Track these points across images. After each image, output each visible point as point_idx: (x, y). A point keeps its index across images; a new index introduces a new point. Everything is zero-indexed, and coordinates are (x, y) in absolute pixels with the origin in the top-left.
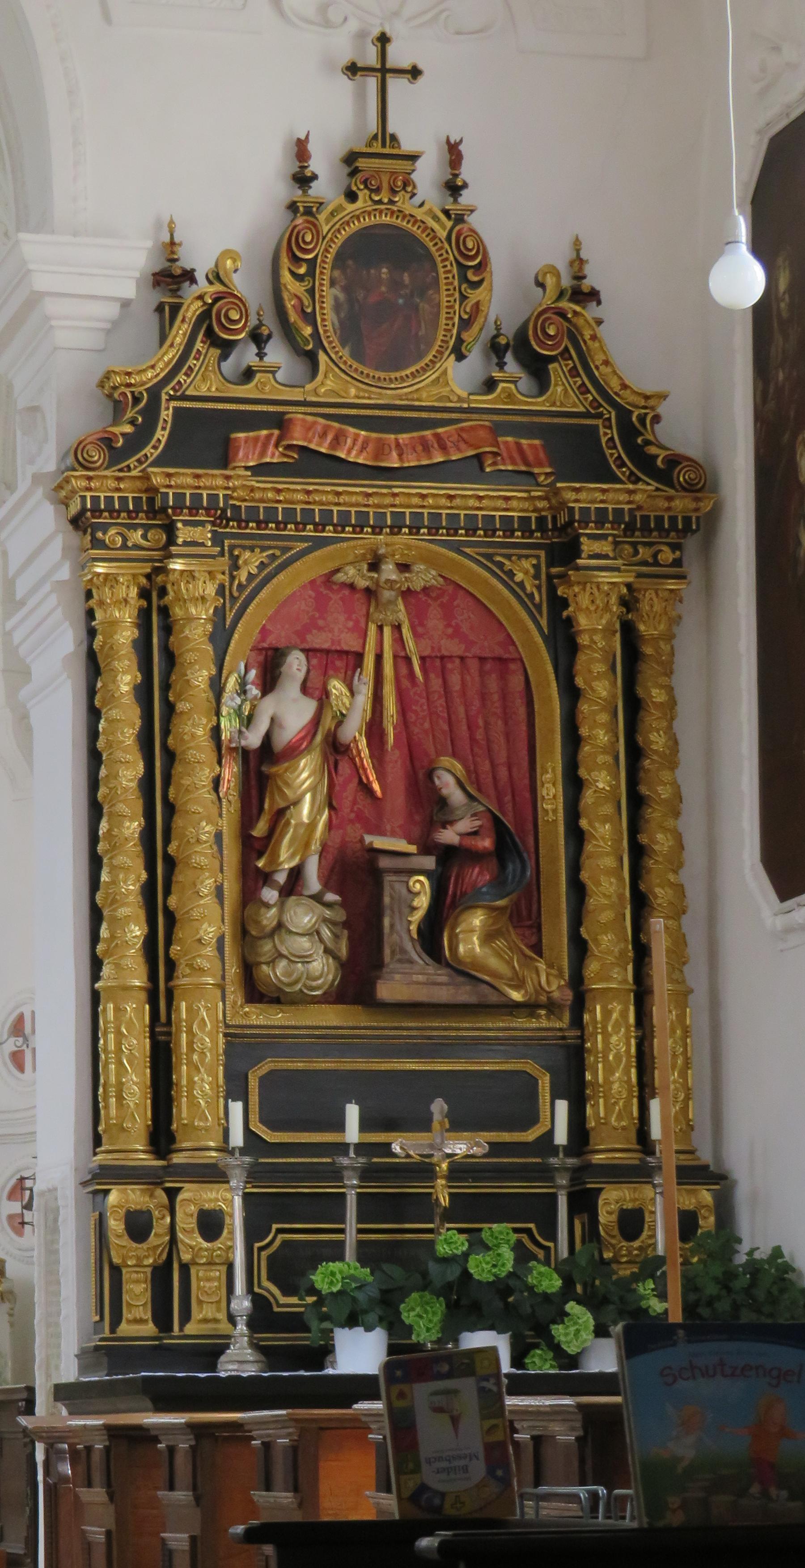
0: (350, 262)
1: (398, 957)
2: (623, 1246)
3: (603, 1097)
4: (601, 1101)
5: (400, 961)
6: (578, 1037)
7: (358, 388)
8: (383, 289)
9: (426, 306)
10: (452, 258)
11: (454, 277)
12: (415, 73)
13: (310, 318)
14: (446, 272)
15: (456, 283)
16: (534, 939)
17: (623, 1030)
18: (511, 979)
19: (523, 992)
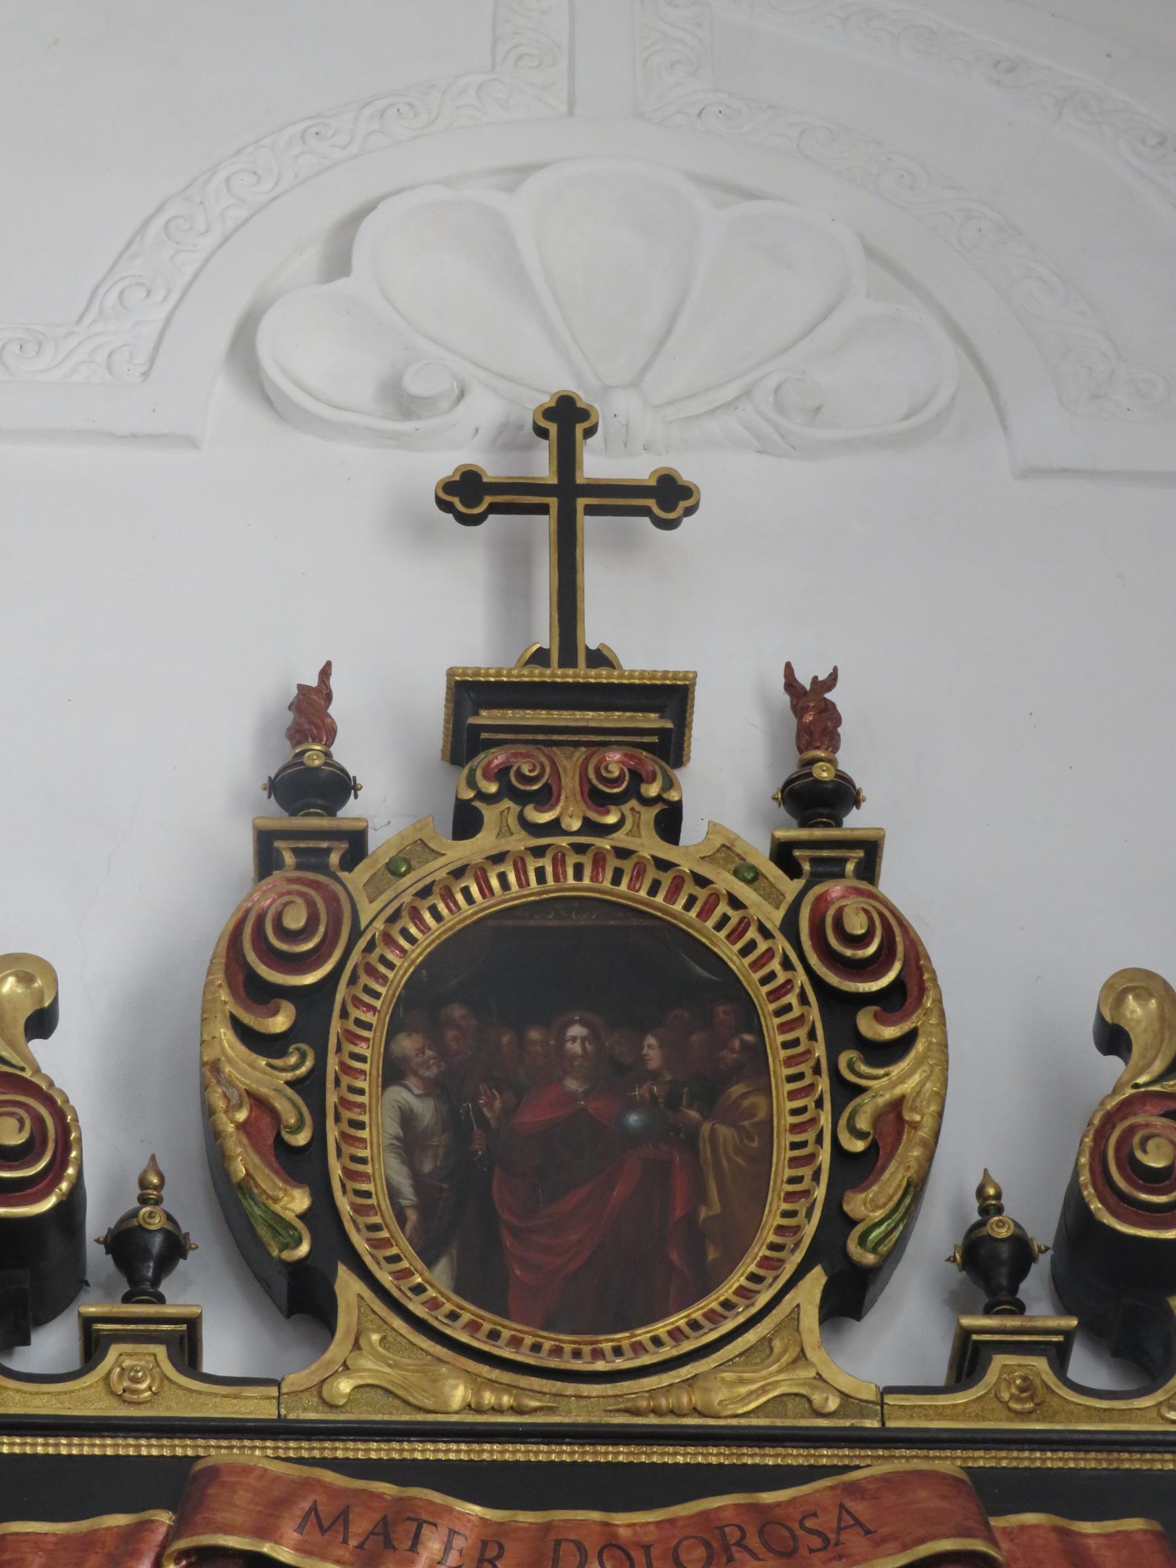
0: (457, 1012)
7: (472, 1377)
8: (572, 1085)
9: (725, 1132)
10: (801, 978)
11: (812, 1036)
12: (669, 498)
13: (303, 1165)
14: (789, 1032)
15: (820, 1051)
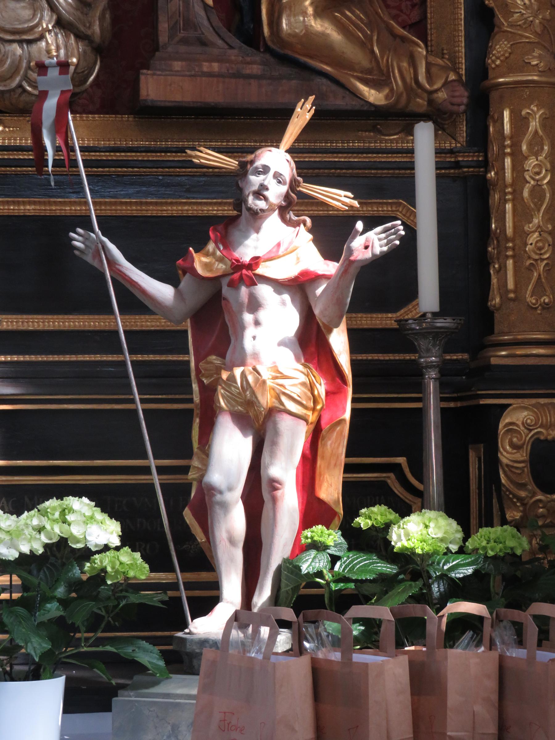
1: (182, 34)
2: (540, 501)
3: (513, 257)
4: (510, 263)
5: (185, 41)
6: (478, 165)
16: (415, 16)
17: (546, 148)
18: (369, 71)
19: (387, 91)
